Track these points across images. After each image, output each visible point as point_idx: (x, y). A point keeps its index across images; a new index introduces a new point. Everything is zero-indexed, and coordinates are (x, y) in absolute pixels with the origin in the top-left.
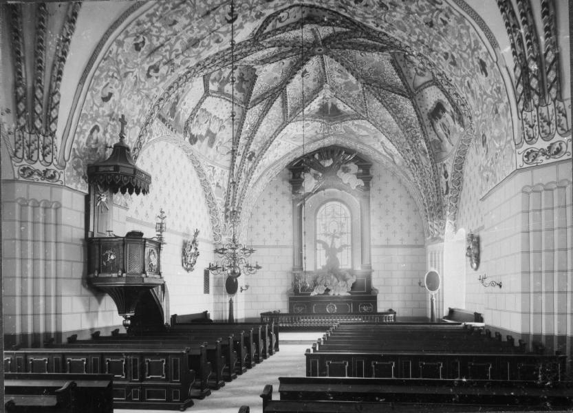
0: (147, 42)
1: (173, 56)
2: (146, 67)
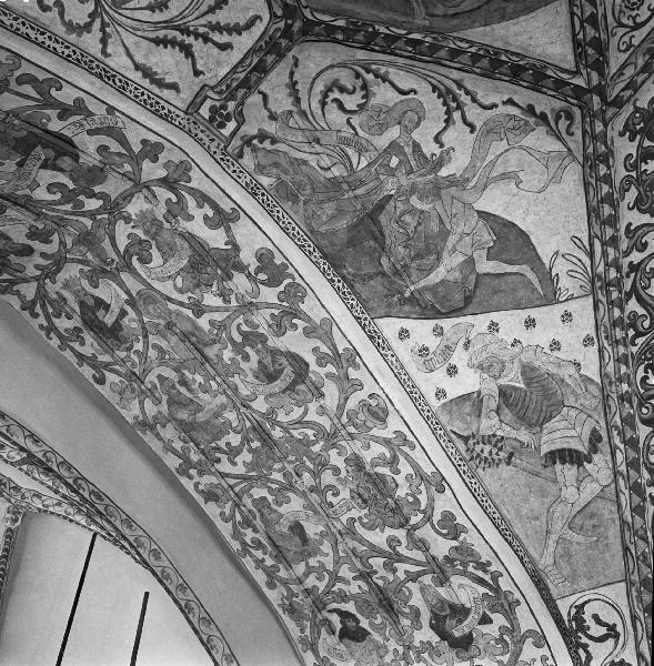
0: (350, 607)
1: (418, 555)
2: (425, 634)
